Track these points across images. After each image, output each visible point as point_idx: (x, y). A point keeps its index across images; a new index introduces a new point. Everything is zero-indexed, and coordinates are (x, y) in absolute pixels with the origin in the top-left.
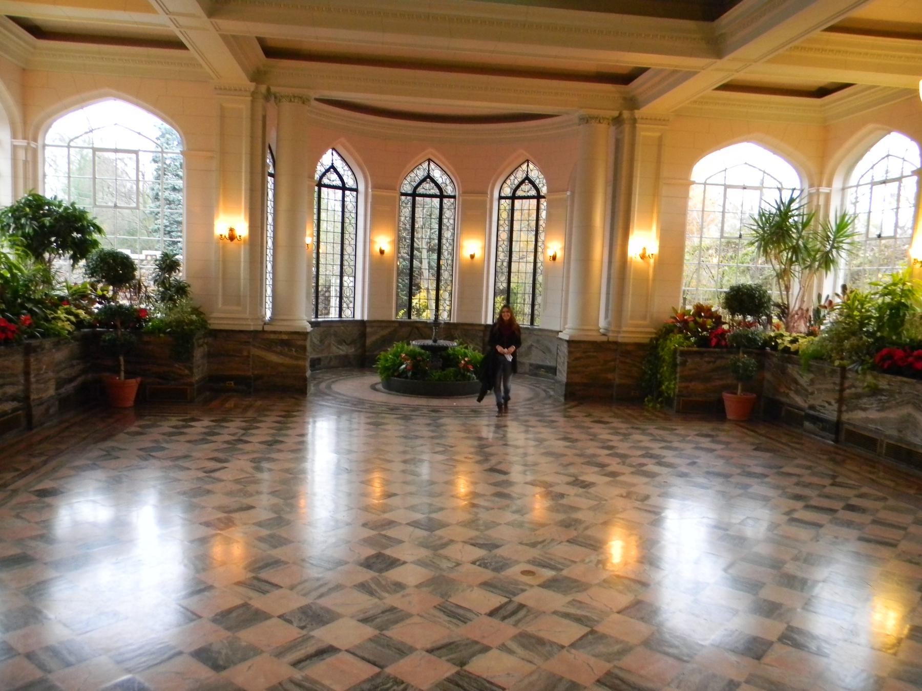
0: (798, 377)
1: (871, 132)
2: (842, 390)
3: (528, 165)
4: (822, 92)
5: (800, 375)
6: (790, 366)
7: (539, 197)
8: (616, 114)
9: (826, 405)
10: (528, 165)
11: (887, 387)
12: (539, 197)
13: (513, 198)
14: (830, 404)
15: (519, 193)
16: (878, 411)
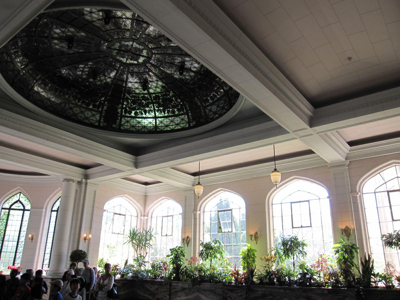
0: (150, 288)
1: (163, 199)
2: (170, 290)
3: (20, 195)
4: (146, 184)
5: (151, 287)
6: (145, 284)
7: (24, 210)
8: (80, 180)
9: (164, 297)
10: (20, 195)
11: (188, 287)
12: (24, 210)
13: (10, 209)
14: (165, 296)
15: (12, 207)
16: (185, 296)
